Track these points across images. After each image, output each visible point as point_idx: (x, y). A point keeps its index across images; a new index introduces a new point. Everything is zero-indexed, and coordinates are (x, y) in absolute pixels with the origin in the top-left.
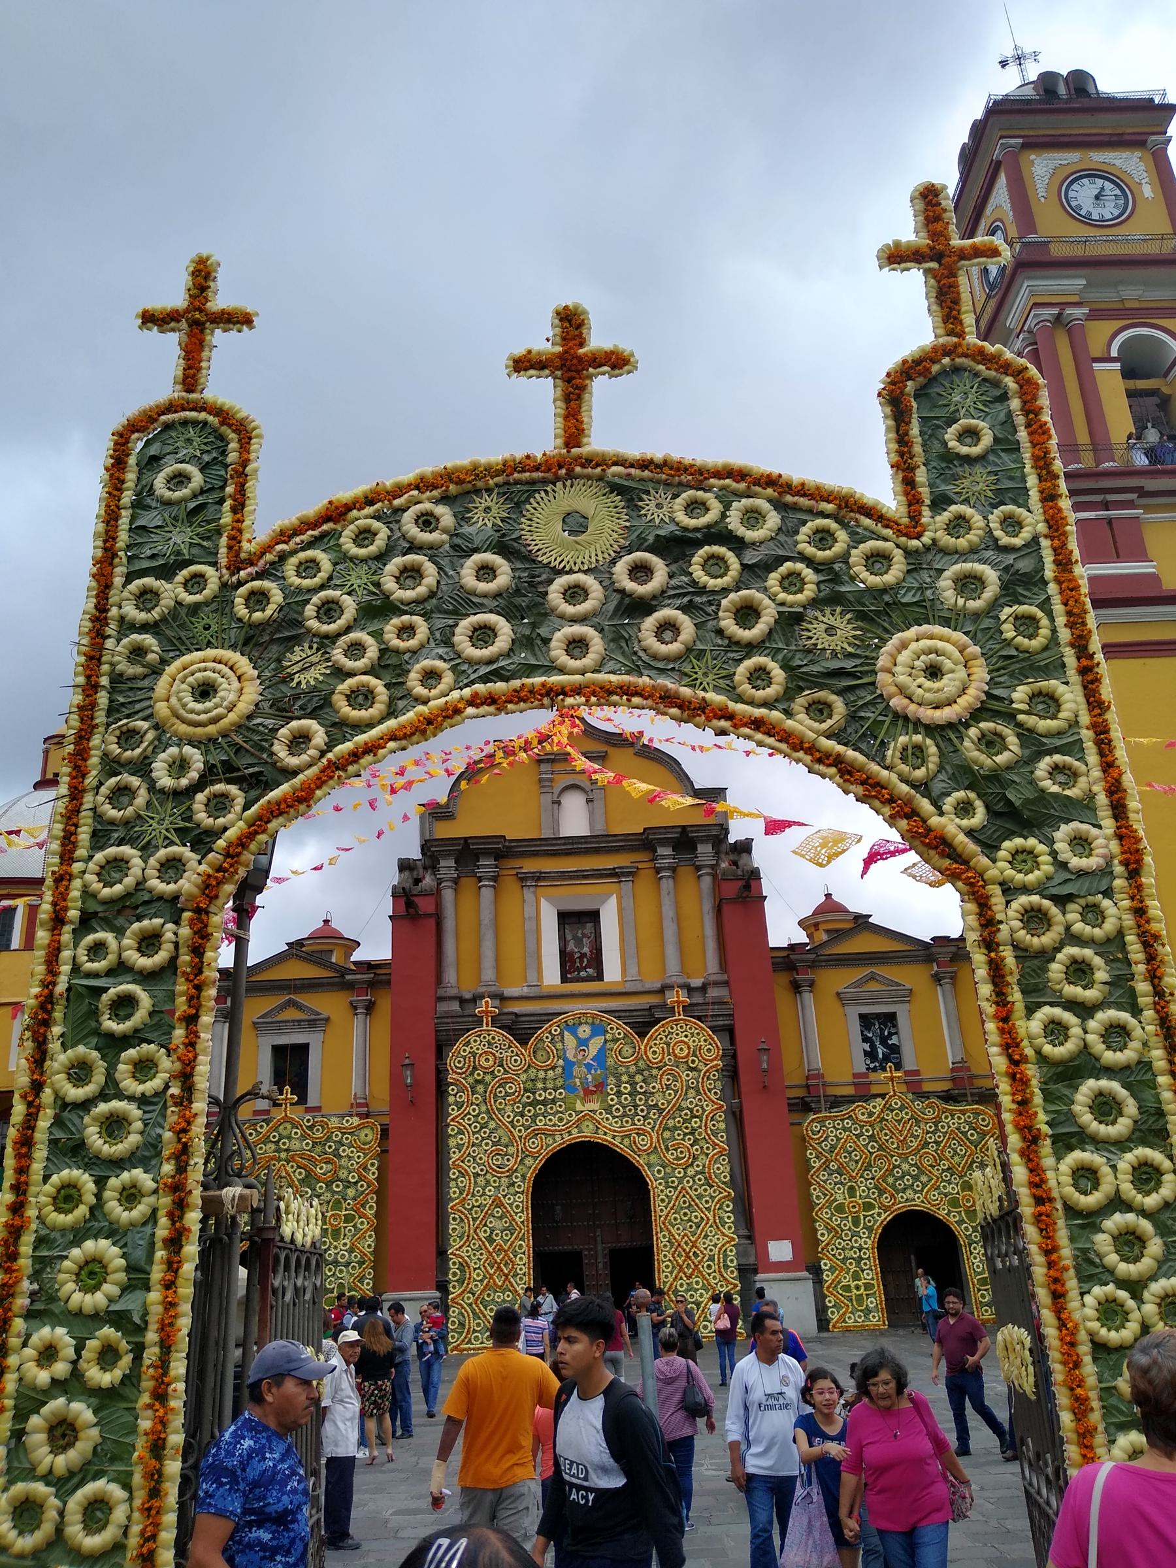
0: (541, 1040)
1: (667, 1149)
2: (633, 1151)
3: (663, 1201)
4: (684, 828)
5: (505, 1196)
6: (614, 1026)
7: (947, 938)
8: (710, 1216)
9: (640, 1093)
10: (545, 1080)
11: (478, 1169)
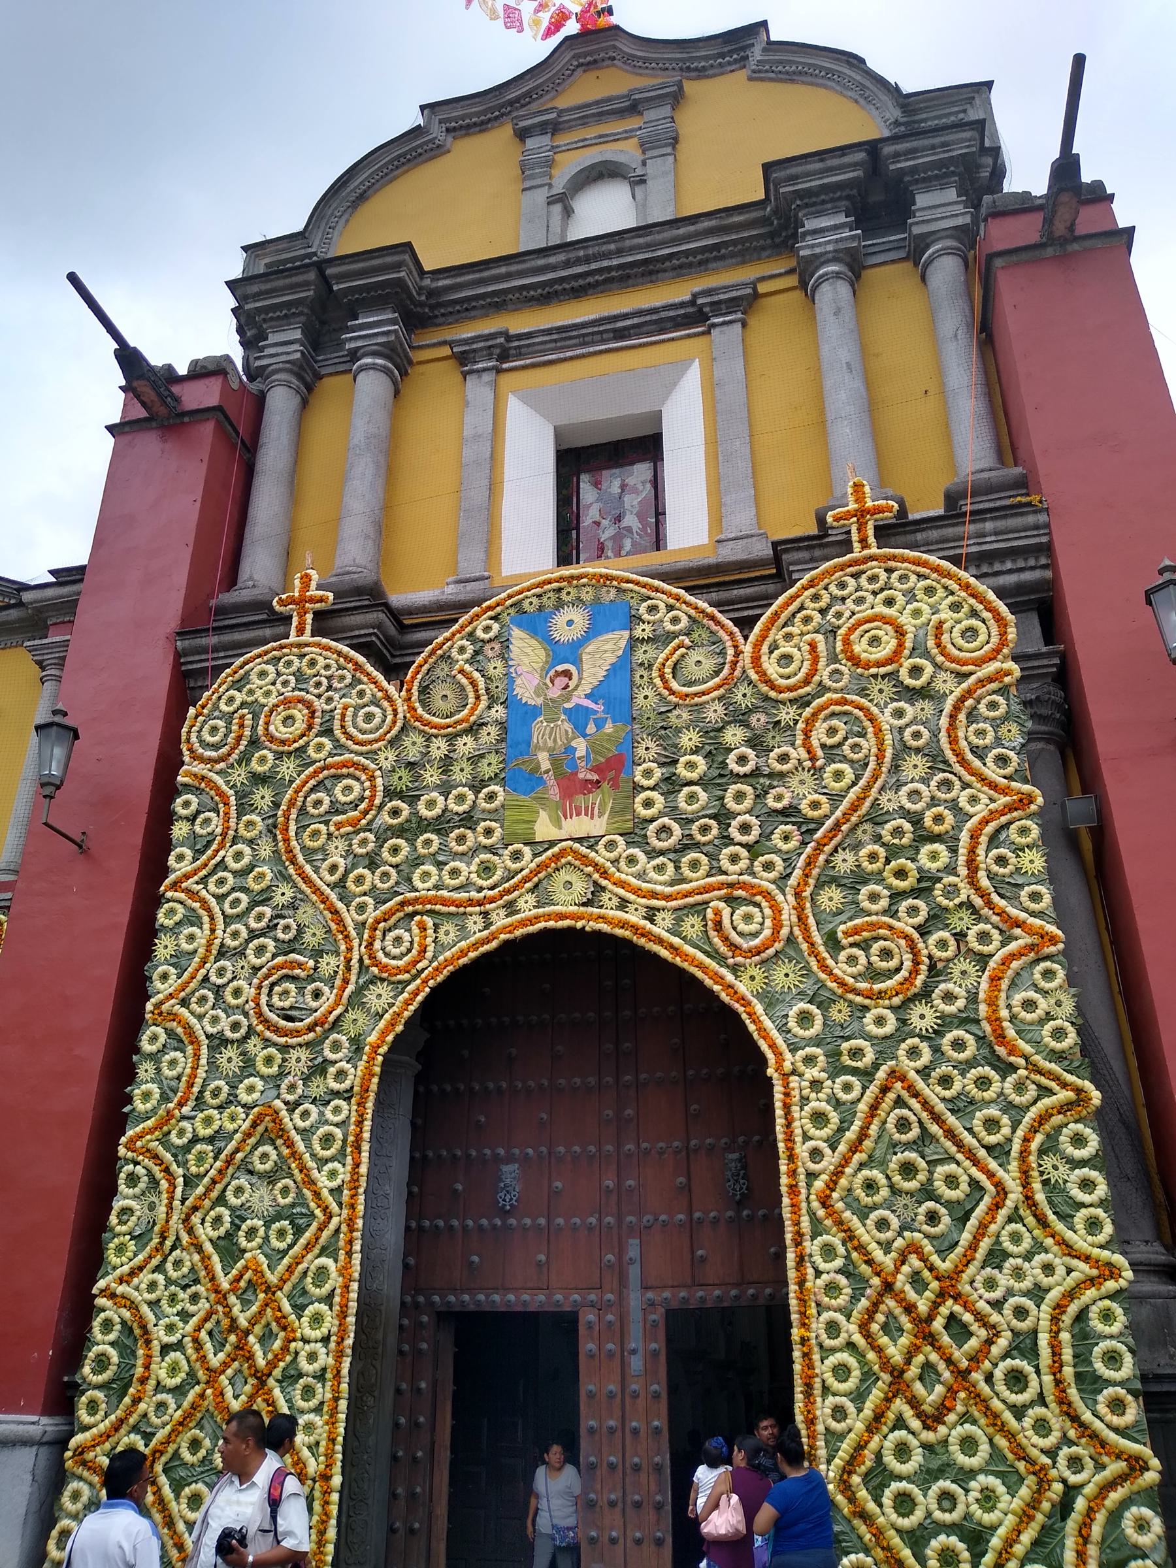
0: (446, 658)
1: (833, 943)
2: (714, 954)
3: (819, 1118)
5: (292, 1107)
6: (660, 601)
8: (1010, 1177)
9: (739, 778)
10: (446, 764)
11: (225, 1024)
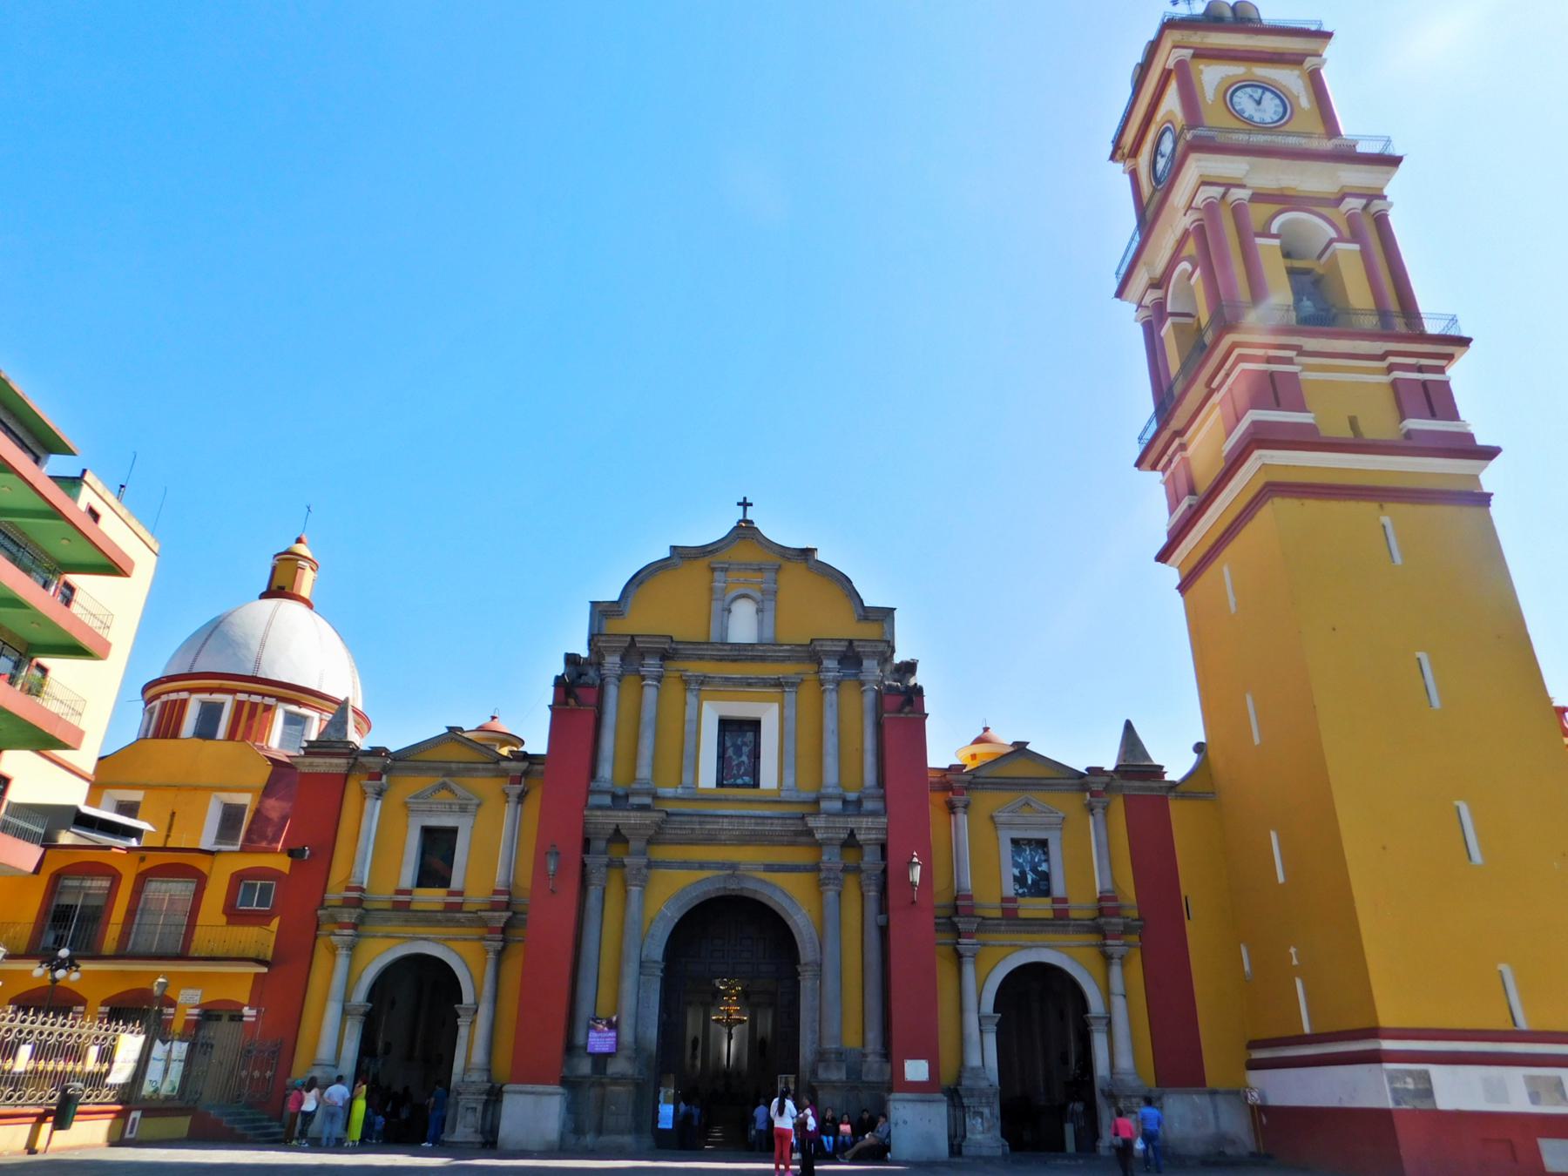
4: (851, 642)
7: (1101, 769)
